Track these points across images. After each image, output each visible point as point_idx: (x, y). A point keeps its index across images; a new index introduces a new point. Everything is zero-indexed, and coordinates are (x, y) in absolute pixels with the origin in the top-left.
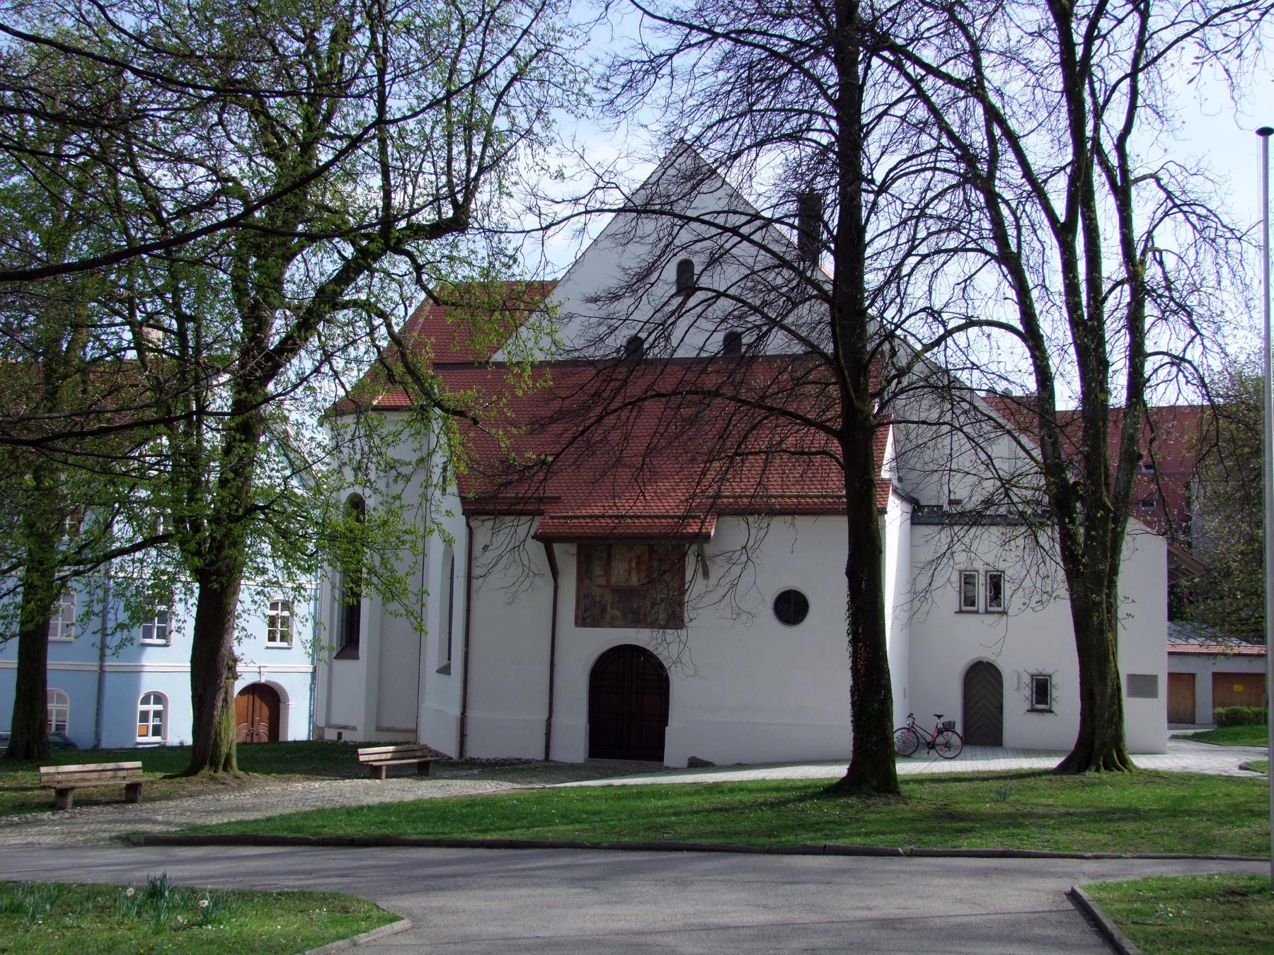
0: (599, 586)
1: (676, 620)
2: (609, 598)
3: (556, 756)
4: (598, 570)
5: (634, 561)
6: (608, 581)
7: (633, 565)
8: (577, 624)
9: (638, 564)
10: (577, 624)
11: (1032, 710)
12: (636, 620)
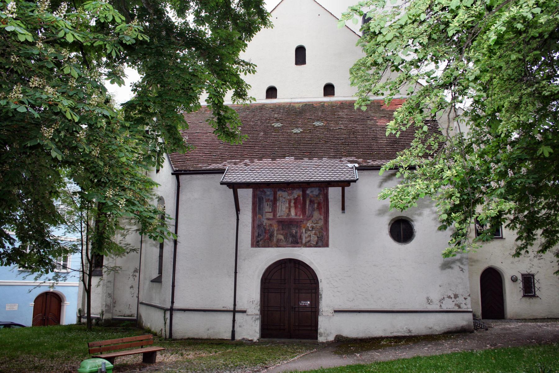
0: (268, 219)
1: (322, 241)
2: (275, 227)
3: (238, 337)
4: (267, 208)
5: (293, 201)
6: (274, 215)
7: (292, 204)
8: (253, 246)
9: (295, 203)
10: (253, 246)
11: (524, 296)
12: (296, 242)
